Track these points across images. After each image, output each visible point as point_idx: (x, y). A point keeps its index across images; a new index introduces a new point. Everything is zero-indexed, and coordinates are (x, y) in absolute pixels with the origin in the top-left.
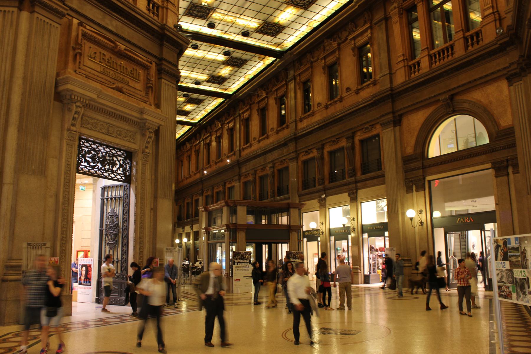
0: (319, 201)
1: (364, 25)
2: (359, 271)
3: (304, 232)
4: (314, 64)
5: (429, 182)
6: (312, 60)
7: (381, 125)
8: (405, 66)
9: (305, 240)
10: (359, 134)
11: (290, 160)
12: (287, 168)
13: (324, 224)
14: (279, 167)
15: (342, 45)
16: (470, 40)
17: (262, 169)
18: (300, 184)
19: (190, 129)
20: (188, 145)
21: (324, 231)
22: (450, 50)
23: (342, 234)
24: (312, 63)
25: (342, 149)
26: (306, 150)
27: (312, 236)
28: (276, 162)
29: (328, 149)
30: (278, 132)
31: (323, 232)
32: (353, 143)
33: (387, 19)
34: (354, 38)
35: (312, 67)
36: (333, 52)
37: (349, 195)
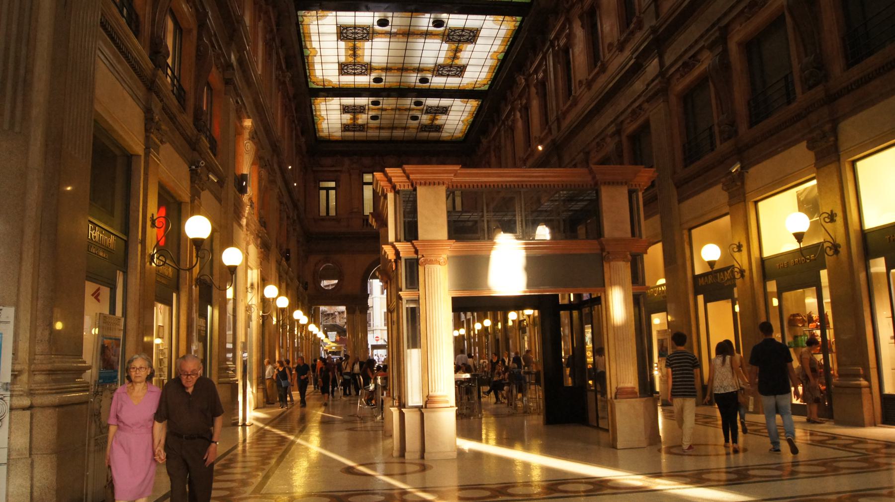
0: (727, 188)
2: (864, 383)
3: (696, 278)
9: (701, 298)
11: (648, 101)
12: (646, 126)
13: (744, 249)
14: (631, 128)
19: (480, 109)
20: (484, 141)
21: (745, 266)
23: (798, 270)
26: (686, 58)
27: (716, 283)
28: (622, 118)
29: (739, 34)
30: (621, 48)
31: (742, 272)
37: (810, 148)
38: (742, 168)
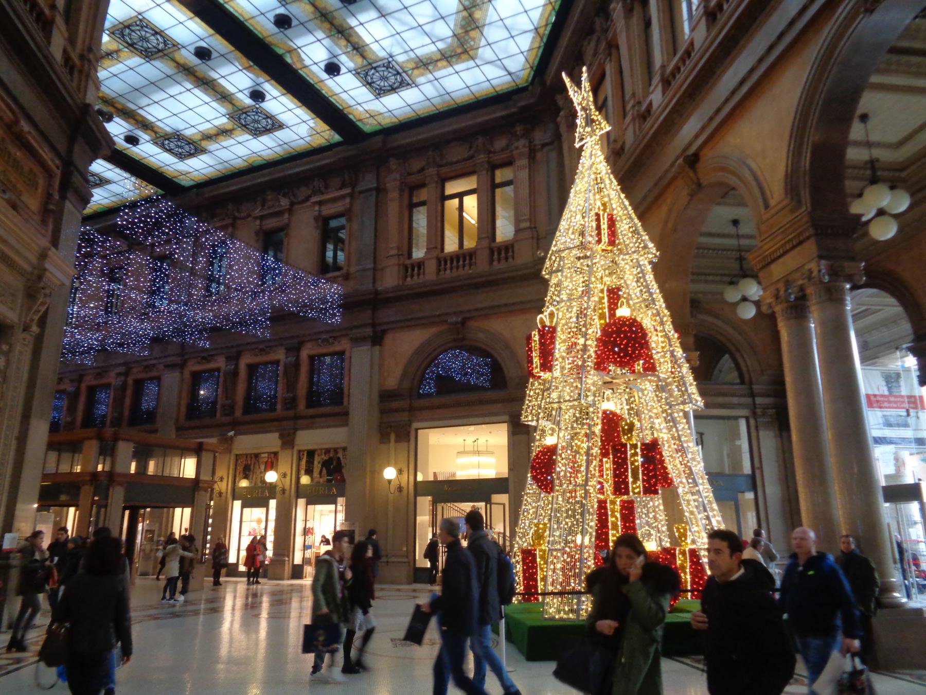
1: (340, 189)
4: (239, 222)
5: (417, 430)
6: (237, 214)
7: (352, 339)
8: (399, 265)
10: (309, 345)
15: (296, 207)
16: (496, 253)
17: (98, 374)
18: (183, 409)
22: (468, 258)
24: (235, 219)
25: (277, 362)
32: (298, 357)
33: (380, 190)
34: (320, 203)
35: (233, 225)
36: (280, 213)
38: (235, 435)
